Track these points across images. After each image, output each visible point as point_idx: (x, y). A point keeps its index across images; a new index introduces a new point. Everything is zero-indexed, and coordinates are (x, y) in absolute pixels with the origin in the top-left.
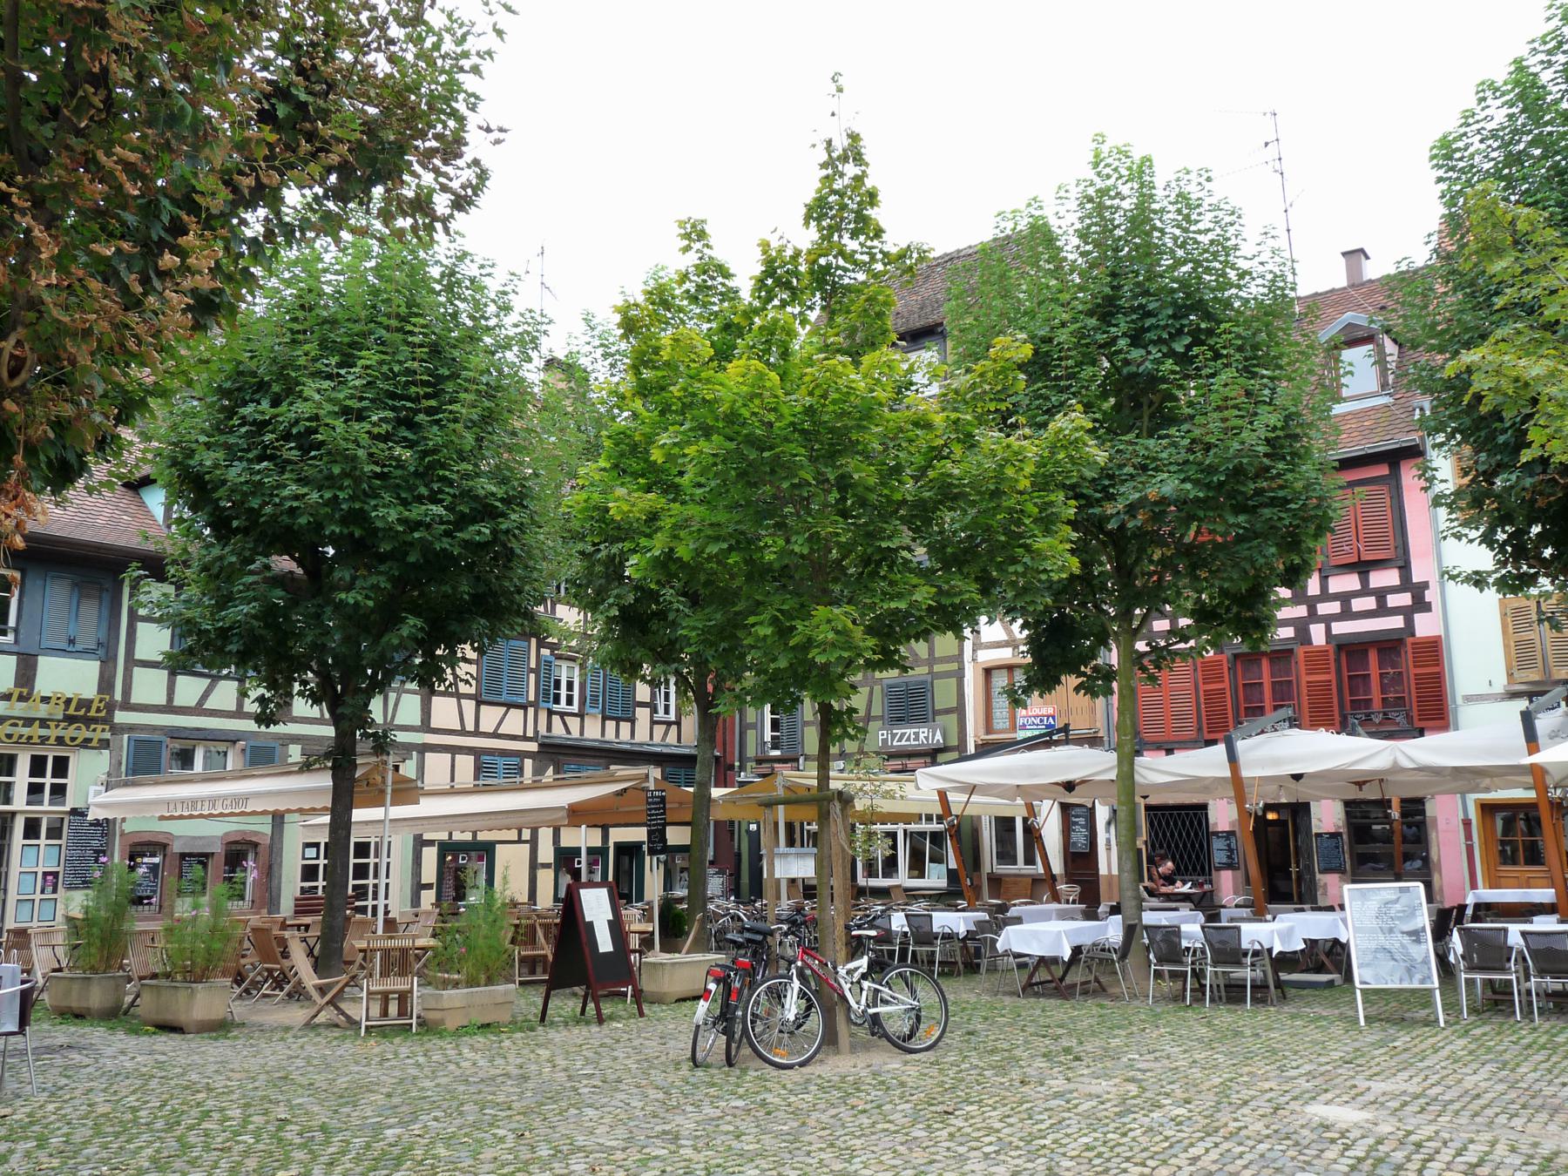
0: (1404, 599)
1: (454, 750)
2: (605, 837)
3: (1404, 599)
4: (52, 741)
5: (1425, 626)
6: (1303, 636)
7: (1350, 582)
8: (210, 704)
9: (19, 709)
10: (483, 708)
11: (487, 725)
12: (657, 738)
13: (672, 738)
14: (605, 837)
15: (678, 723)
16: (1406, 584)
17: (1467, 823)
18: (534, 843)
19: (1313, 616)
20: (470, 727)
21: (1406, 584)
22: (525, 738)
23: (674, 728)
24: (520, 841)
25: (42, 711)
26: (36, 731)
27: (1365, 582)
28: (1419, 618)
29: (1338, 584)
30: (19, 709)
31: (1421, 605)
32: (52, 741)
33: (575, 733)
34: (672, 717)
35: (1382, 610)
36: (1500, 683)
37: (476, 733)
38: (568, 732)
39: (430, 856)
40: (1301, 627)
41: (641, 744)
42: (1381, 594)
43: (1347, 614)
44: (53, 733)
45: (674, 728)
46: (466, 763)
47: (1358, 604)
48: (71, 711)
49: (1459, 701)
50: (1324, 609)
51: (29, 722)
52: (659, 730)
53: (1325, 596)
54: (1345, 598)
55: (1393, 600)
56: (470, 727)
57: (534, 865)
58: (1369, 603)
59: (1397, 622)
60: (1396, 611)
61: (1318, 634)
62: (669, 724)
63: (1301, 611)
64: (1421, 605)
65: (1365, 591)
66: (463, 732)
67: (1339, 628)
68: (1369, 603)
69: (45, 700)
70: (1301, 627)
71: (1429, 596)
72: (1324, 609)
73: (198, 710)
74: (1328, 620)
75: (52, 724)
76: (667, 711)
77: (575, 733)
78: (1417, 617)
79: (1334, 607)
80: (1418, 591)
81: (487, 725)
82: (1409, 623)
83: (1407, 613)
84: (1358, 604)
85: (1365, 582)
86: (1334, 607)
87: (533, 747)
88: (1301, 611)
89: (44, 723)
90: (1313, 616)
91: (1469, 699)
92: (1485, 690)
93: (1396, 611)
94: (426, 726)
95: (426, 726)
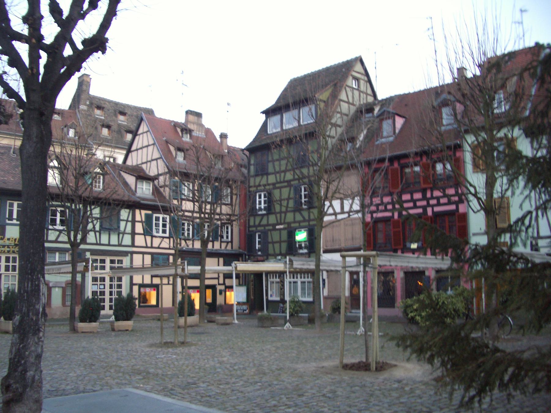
1: (143, 253)
3: (456, 198)
4: (11, 252)
5: (462, 208)
10: (154, 239)
11: (156, 244)
13: (229, 247)
15: (232, 242)
16: (457, 194)
19: (428, 205)
20: (149, 245)
22: (169, 249)
23: (230, 244)
24: (169, 284)
25: (7, 243)
26: (6, 249)
31: (461, 201)
32: (11, 252)
33: (191, 246)
34: (230, 239)
37: (152, 247)
38: (188, 246)
40: (424, 208)
41: (216, 250)
43: (439, 204)
44: (12, 249)
45: (230, 244)
46: (148, 258)
47: (442, 201)
48: (16, 243)
49: (471, 235)
52: (224, 245)
53: (432, 198)
54: (438, 198)
56: (149, 245)
59: (453, 207)
60: (420, 207)
61: (429, 211)
62: (228, 242)
63: (424, 203)
66: (147, 247)
67: (436, 209)
69: (9, 239)
70: (424, 208)
73: (56, 241)
74: (433, 206)
75: (11, 247)
76: (227, 237)
77: (191, 246)
81: (156, 244)
87: (173, 252)
88: (424, 203)
89: (8, 247)
90: (428, 205)
91: (474, 234)
92: (477, 231)
93: (420, 207)
94: (133, 245)
95: (133, 245)
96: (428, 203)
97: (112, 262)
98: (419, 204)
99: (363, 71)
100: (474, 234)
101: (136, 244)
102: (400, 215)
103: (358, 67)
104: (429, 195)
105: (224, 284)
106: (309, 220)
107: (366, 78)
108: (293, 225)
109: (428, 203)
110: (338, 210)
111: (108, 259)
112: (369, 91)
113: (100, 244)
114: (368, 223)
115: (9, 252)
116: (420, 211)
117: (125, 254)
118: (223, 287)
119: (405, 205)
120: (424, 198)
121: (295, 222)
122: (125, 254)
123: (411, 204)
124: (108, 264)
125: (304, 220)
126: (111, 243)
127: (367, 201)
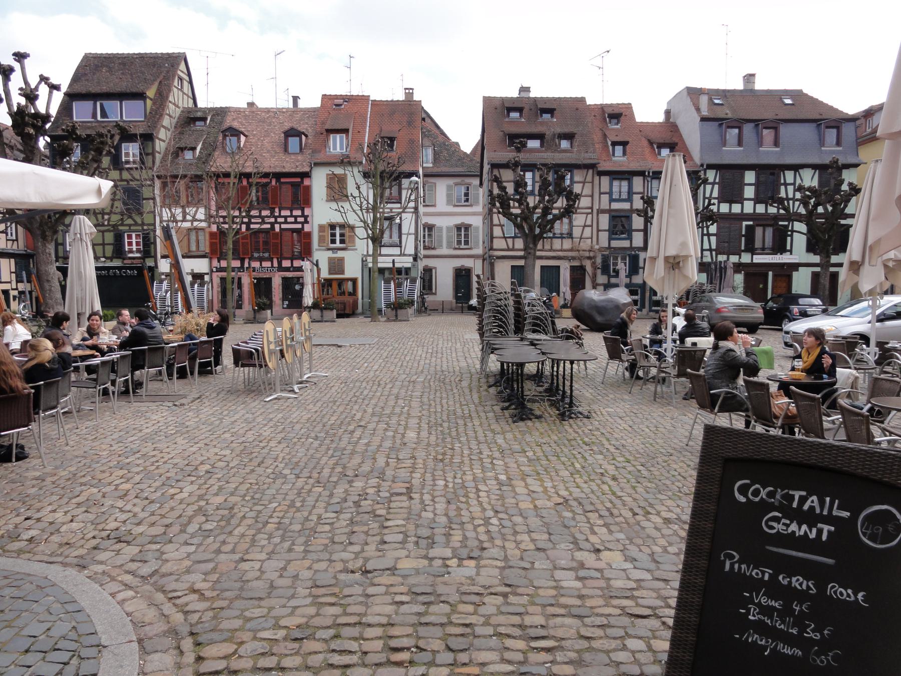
5: (307, 228)
6: (273, 228)
7: (287, 213)
12: (9, 247)
13: (15, 247)
15: (17, 240)
16: (303, 215)
17: (314, 284)
19: (276, 222)
27: (291, 213)
29: (284, 213)
31: (306, 222)
34: (14, 238)
35: (296, 222)
40: (272, 224)
42: (296, 217)
43: (286, 222)
47: (289, 220)
50: (279, 220)
53: (280, 216)
54: (286, 217)
55: (299, 220)
58: (292, 220)
59: (299, 226)
61: (277, 227)
62: (13, 241)
63: (272, 220)
64: (306, 222)
65: (291, 216)
67: (283, 226)
68: (292, 220)
70: (272, 224)
71: (309, 219)
72: (279, 220)
74: (280, 223)
79: (282, 220)
80: (306, 217)
84: (289, 220)
85: (291, 213)
86: (282, 220)
88: (272, 220)
90: (276, 222)
98: (267, 220)
99: (185, 71)
102: (248, 228)
103: (182, 66)
104: (277, 214)
105: (17, 289)
106: (143, 224)
107: (187, 78)
108: (121, 228)
110: (180, 218)
112: (190, 94)
114: (215, 233)
116: (268, 226)
118: (16, 293)
120: (272, 215)
125: (136, 224)
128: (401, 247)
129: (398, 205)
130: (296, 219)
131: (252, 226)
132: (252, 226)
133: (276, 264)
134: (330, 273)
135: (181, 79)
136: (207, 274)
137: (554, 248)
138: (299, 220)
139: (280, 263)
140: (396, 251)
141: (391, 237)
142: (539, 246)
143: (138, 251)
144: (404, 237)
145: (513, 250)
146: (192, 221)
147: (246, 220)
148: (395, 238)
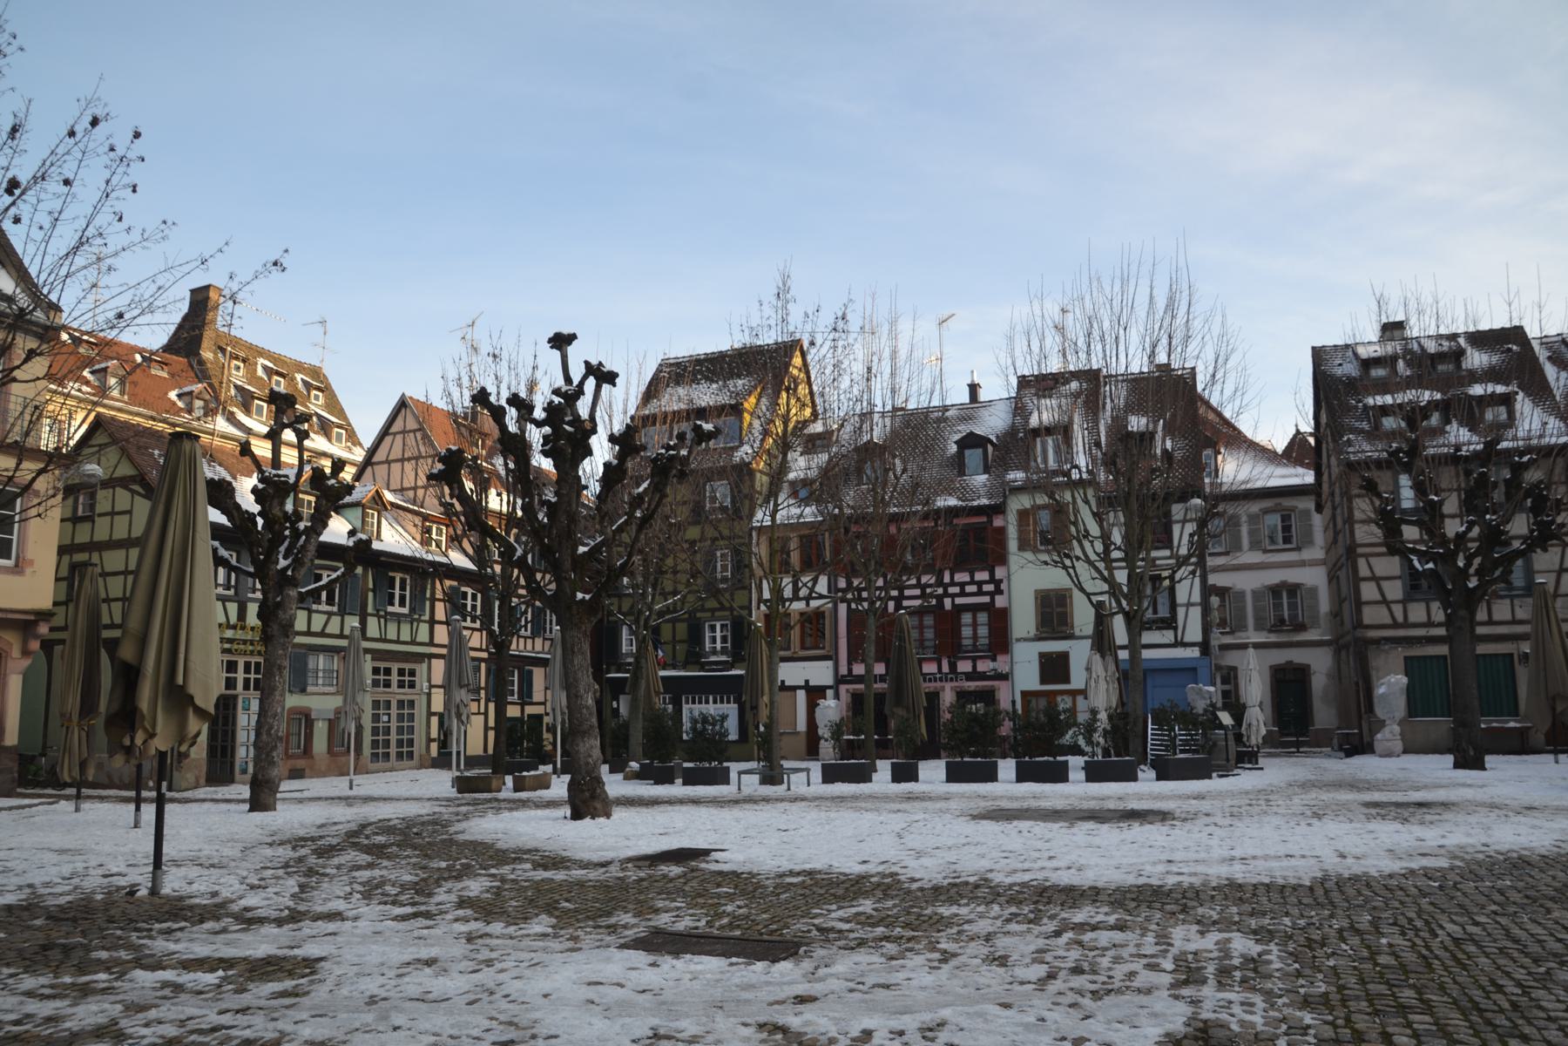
0: (990, 588)
2: (523, 711)
3: (990, 588)
5: (1000, 601)
8: (328, 631)
9: (240, 635)
14: (523, 711)
16: (992, 580)
18: (486, 714)
19: (946, 594)
21: (992, 580)
22: (480, 650)
27: (972, 577)
28: (997, 598)
30: (240, 635)
31: (999, 591)
35: (980, 593)
36: (1033, 632)
39: (435, 720)
40: (940, 599)
42: (980, 584)
43: (963, 594)
47: (969, 589)
50: (952, 590)
51: (245, 642)
53: (953, 584)
54: (962, 585)
55: (986, 588)
57: (486, 728)
59: (986, 599)
61: (948, 603)
63: (940, 591)
64: (999, 591)
65: (972, 582)
67: (958, 601)
71: (1003, 586)
72: (952, 590)
74: (953, 596)
78: (997, 598)
79: (956, 590)
80: (998, 583)
82: (993, 600)
83: (992, 594)
84: (969, 589)
85: (972, 577)
86: (956, 590)
87: (485, 655)
90: (946, 594)
91: (1018, 640)
92: (1024, 635)
94: (431, 643)
95: (431, 643)
96: (945, 590)
97: (401, 672)
100: (1018, 640)
101: (436, 641)
102: (898, 607)
103: (797, 361)
104: (947, 579)
109: (945, 590)
110: (788, 593)
111: (395, 667)
113: (386, 641)
115: (252, 653)
117: (420, 658)
119: (907, 593)
120: (940, 583)
121: (703, 610)
122: (420, 658)
123: (917, 592)
124: (395, 678)
125: (722, 608)
126: (436, 641)
127: (842, 583)
128: (1175, 629)
129: (1167, 553)
130: (980, 588)
131: (906, 603)
132: (906, 603)
133: (946, 669)
134: (1043, 682)
135: (795, 380)
136: (830, 687)
137: (1496, 617)
138: (986, 588)
139: (953, 667)
140: (1168, 636)
141: (1155, 612)
142: (1481, 615)
143: (724, 651)
144: (1181, 612)
145: (1406, 624)
146: (808, 599)
147: (894, 593)
148: (1163, 612)
